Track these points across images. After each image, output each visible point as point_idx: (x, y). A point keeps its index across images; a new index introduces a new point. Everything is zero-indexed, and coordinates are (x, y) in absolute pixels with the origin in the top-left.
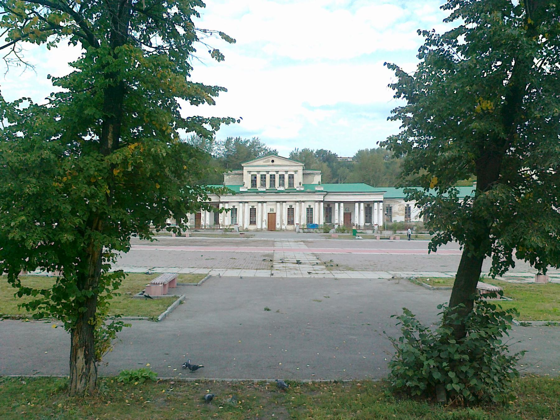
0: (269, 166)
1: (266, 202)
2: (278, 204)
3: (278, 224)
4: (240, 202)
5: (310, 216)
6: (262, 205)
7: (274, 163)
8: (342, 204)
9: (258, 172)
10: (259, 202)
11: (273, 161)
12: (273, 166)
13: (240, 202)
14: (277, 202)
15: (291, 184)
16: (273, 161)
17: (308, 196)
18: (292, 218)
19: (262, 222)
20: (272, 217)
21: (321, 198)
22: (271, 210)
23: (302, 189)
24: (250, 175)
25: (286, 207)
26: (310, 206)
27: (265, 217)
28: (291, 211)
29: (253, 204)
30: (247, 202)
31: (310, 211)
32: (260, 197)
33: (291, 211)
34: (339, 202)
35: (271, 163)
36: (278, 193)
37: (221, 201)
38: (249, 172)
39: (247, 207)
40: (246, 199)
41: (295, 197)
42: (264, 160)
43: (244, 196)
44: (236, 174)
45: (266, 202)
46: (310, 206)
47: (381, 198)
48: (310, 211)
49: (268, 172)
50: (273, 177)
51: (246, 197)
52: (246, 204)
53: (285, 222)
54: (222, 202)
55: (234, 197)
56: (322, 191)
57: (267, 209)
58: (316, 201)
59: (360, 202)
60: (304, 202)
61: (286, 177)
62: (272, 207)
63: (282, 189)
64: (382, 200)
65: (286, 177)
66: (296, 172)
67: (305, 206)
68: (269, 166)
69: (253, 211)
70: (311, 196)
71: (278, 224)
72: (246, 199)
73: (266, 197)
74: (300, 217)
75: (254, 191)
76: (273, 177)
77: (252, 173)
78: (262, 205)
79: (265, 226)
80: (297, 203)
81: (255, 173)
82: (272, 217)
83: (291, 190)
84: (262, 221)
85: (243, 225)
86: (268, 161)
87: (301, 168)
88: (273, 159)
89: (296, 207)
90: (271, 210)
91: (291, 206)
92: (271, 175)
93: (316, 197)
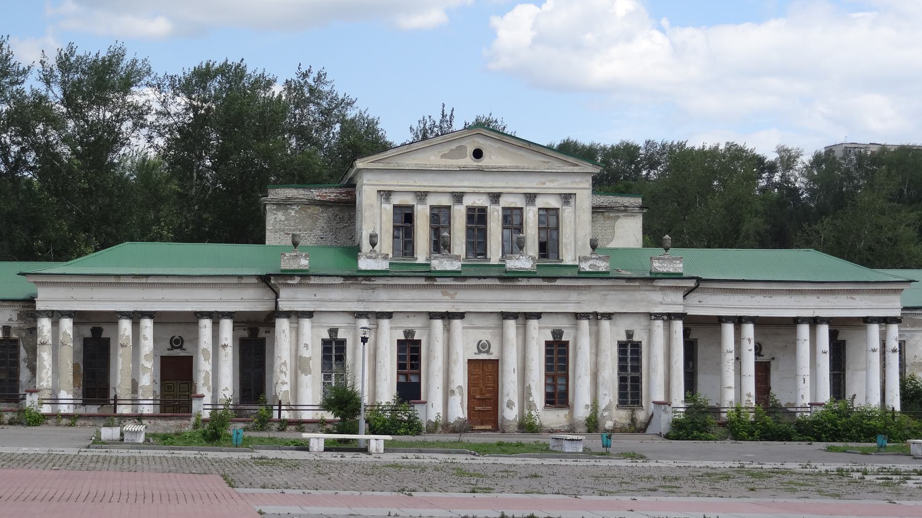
0: (464, 171)
1: (461, 316)
2: (511, 324)
3: (510, 405)
5: (629, 373)
7: (485, 162)
8: (749, 330)
9: (422, 196)
10: (433, 316)
11: (478, 154)
12: (480, 170)
14: (505, 316)
15: (547, 248)
16: (478, 154)
17: (623, 296)
18: (560, 381)
20: (485, 375)
21: (674, 302)
22: (483, 347)
23: (602, 266)
24: (388, 208)
25: (539, 334)
26: (630, 334)
27: (460, 378)
28: (558, 354)
29: (410, 324)
31: (630, 353)
32: (437, 295)
33: (558, 354)
34: (739, 322)
35: (469, 161)
36: (509, 278)
37: (284, 306)
38: (386, 195)
39: (388, 337)
41: (574, 296)
42: (446, 150)
43: (374, 288)
44: (313, 203)
45: (461, 316)
46: (630, 334)
47: (891, 306)
48: (630, 353)
50: (477, 218)
51: (383, 295)
53: (538, 397)
54: (288, 314)
55: (336, 294)
56: (678, 276)
57: (465, 342)
58: (658, 316)
59: (814, 322)
60: (608, 316)
61: (531, 217)
62: (485, 336)
63: (522, 263)
64: (897, 313)
65: (531, 217)
66: (567, 198)
67: (612, 334)
68: (464, 171)
69: (410, 354)
70: (638, 295)
71: (510, 405)
72: (382, 300)
73: (462, 295)
74: (595, 376)
75: (405, 271)
76: (477, 218)
77: (397, 200)
78: (448, 329)
79: (459, 411)
80: (585, 324)
81: (409, 200)
82: (485, 375)
83: (550, 269)
84: (448, 392)
86: (459, 152)
87: (587, 183)
88: (481, 143)
89: (582, 342)
90: (483, 347)
92: (470, 209)
93: (657, 296)
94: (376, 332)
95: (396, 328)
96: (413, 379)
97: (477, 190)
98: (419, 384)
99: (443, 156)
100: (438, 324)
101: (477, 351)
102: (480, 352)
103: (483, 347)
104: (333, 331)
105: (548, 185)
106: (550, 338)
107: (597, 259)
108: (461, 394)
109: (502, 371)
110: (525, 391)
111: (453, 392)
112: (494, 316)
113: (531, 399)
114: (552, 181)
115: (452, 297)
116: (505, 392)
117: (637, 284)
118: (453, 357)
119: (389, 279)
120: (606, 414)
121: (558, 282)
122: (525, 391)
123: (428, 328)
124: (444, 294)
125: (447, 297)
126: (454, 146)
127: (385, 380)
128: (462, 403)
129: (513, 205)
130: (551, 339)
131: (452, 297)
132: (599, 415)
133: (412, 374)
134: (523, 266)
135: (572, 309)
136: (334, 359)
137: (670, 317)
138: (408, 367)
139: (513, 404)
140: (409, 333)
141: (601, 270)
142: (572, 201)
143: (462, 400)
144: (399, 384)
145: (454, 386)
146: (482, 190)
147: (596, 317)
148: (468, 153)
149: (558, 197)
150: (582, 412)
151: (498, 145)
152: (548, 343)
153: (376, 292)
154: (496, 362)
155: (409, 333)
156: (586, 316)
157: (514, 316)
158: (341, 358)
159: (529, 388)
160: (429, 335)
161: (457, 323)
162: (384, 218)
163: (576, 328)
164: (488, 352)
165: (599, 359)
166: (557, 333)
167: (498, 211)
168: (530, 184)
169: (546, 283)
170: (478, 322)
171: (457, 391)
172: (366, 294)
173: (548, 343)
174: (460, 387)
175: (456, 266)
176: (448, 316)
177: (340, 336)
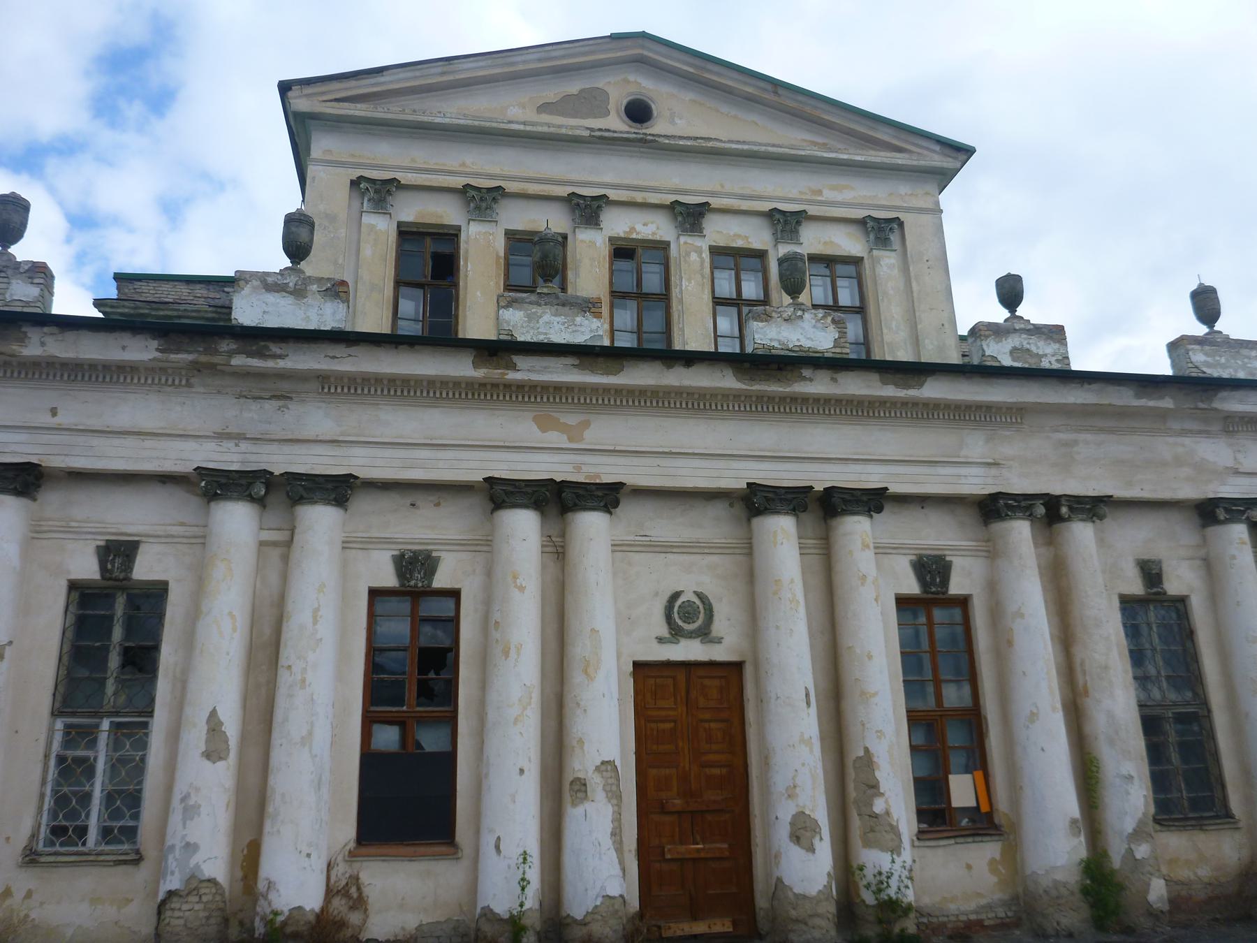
3: (802, 832)
4: (216, 485)
6: (558, 552)
7: (659, 127)
10: (500, 494)
13: (216, 485)
17: (1121, 447)
19: (548, 795)
20: (694, 723)
22: (685, 616)
24: (382, 228)
27: (606, 729)
30: (338, 490)
32: (517, 425)
39: (333, 577)
40: (314, 436)
41: (975, 444)
42: (553, 91)
49: (588, 209)
51: (317, 418)
52: (320, 521)
70: (1165, 446)
72: (314, 436)
73: (607, 430)
77: (411, 210)
78: (558, 552)
79: (604, 869)
82: (694, 723)
84: (559, 789)
85: (249, 857)
90: (685, 616)
91: (932, 569)
94: (286, 559)
95: (368, 544)
96: (431, 740)
97: (639, 197)
98: (449, 759)
99: (544, 108)
100: (523, 526)
101: (664, 631)
102: (676, 633)
103: (689, 613)
104: (118, 553)
105: (828, 195)
108: (615, 796)
109: (761, 700)
110: (848, 774)
111: (581, 787)
112: (718, 510)
113: (879, 806)
114: (833, 188)
115: (574, 433)
116: (780, 781)
117: (1167, 403)
118: (579, 649)
119: (340, 350)
120: (1142, 851)
122: (848, 774)
123: (485, 546)
124: (545, 424)
125: (555, 438)
126: (573, 87)
127: (307, 739)
128: (616, 834)
129: (739, 243)
130: (911, 586)
131: (574, 433)
132: (1116, 860)
133: (423, 721)
134: (807, 344)
135: (976, 483)
136: (114, 661)
138: (411, 692)
139: (815, 828)
140: (415, 565)
141: (1045, 364)
142: (894, 238)
143: (617, 819)
144: (371, 762)
145: (583, 763)
146: (654, 198)
148: (611, 106)
149: (852, 229)
150: (1056, 850)
151: (689, 96)
153: (295, 409)
154: (735, 669)
155: (415, 565)
156: (1017, 505)
157: (793, 500)
158: (142, 660)
159: (867, 761)
160: (489, 573)
161: (592, 526)
162: (367, 251)
163: (993, 552)
164: (704, 634)
165: (1079, 653)
166: (932, 569)
167: (699, 251)
168: (786, 189)
169: (890, 391)
170: (666, 525)
171: (596, 783)
172: (255, 415)
173: (903, 602)
174: (607, 766)
175: (587, 330)
176: (558, 500)
177: (145, 569)
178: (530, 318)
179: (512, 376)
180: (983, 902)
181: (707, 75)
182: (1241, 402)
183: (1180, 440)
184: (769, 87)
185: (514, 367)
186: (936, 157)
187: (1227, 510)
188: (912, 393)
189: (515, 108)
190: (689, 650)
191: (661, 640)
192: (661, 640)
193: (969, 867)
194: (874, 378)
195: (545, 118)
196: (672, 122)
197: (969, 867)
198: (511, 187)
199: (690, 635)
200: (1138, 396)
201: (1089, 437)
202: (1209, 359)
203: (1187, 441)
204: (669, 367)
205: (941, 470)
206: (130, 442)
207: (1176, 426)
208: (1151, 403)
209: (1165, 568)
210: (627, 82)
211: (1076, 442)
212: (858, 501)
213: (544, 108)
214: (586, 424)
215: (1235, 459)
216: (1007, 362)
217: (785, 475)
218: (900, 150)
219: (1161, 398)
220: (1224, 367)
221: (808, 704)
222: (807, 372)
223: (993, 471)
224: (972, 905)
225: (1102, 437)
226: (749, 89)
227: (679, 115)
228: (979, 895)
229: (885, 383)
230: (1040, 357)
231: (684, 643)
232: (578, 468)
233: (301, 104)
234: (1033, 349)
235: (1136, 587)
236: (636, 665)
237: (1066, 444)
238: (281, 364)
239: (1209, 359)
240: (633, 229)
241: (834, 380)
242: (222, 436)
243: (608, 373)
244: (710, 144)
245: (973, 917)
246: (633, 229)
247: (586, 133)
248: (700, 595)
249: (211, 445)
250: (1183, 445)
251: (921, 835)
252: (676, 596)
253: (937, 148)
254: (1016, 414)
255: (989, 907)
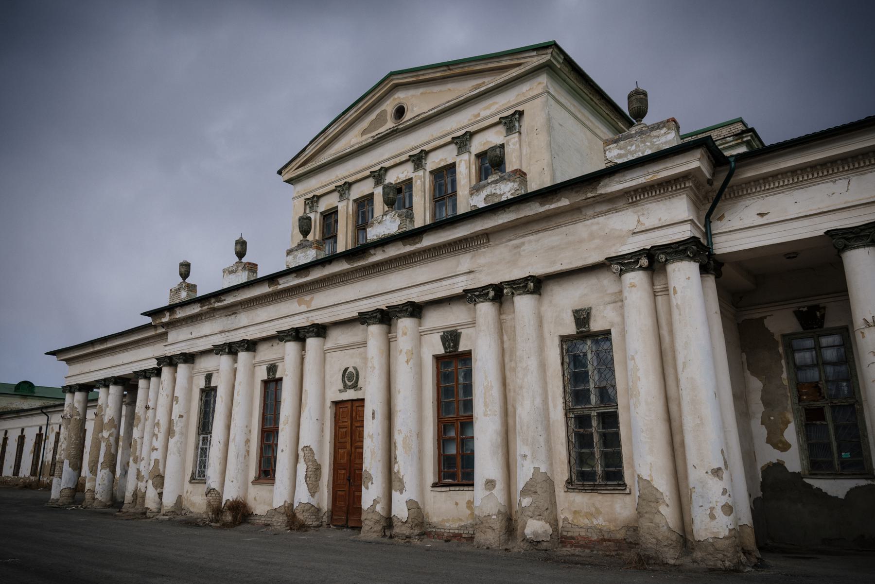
1: (321, 330)
25: (417, 347)
42: (365, 123)
45: (321, 330)
62: (349, 360)
97: (397, 160)
99: (364, 133)
102: (346, 387)
105: (484, 114)
106: (440, 350)
107: (496, 182)
114: (486, 109)
121: (428, 241)
126: (373, 116)
129: (443, 164)
131: (308, 304)
132: (516, 508)
135: (458, 286)
137: (654, 260)
141: (504, 198)
147: (499, 294)
152: (437, 358)
161: (312, 343)
178: (295, 257)
179: (280, 287)
180: (462, 524)
181: (421, 78)
182: (620, 182)
183: (596, 220)
184: (445, 68)
185: (278, 284)
186: (535, 59)
187: (666, 254)
188: (418, 246)
189: (353, 139)
190: (350, 395)
191: (340, 391)
192: (340, 391)
193: (457, 504)
194: (400, 244)
195: (365, 137)
196: (412, 111)
197: (457, 504)
198: (387, 165)
199: (351, 387)
200: (542, 204)
201: (532, 237)
202: (622, 152)
203: (601, 219)
204: (324, 266)
205: (445, 283)
206: (204, 339)
207: (590, 212)
208: (553, 206)
209: (593, 312)
210: (395, 99)
211: (523, 244)
212: (401, 311)
213: (364, 133)
214: (312, 299)
215: (639, 221)
216: (481, 205)
217: (394, 300)
218: (520, 65)
219: (559, 200)
220: (635, 152)
221: (373, 418)
222: (372, 252)
223: (471, 276)
224: (456, 525)
225: (541, 235)
226: (439, 74)
227: (418, 102)
228: (460, 520)
229: (405, 245)
230: (501, 195)
231: (348, 391)
232: (307, 319)
233: (287, 176)
234: (498, 192)
235: (570, 329)
236: (333, 402)
237: (517, 247)
238: (225, 303)
239: (622, 152)
240: (398, 178)
241: (384, 251)
242: (221, 332)
243: (306, 276)
244: (420, 117)
245: (457, 531)
246: (398, 178)
247: (371, 140)
248: (355, 368)
249: (219, 336)
250: (598, 223)
251: (435, 485)
252: (346, 370)
253: (535, 53)
254: (486, 236)
255: (465, 527)
